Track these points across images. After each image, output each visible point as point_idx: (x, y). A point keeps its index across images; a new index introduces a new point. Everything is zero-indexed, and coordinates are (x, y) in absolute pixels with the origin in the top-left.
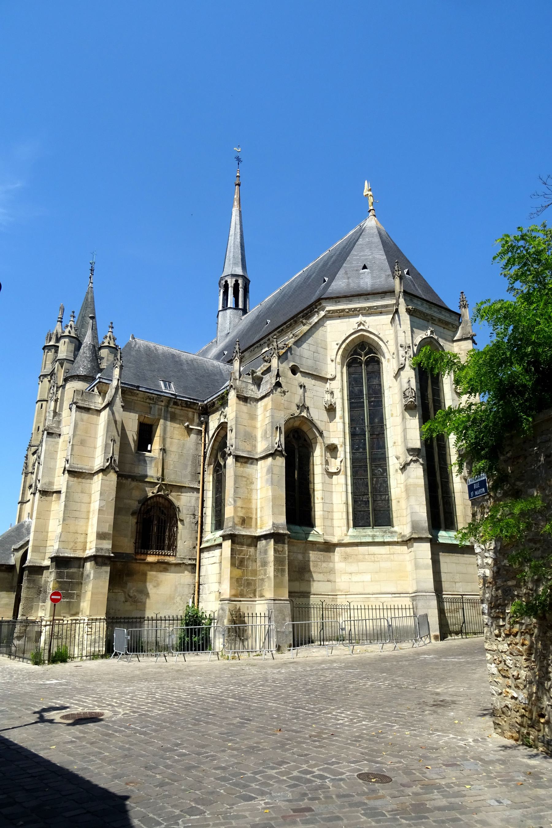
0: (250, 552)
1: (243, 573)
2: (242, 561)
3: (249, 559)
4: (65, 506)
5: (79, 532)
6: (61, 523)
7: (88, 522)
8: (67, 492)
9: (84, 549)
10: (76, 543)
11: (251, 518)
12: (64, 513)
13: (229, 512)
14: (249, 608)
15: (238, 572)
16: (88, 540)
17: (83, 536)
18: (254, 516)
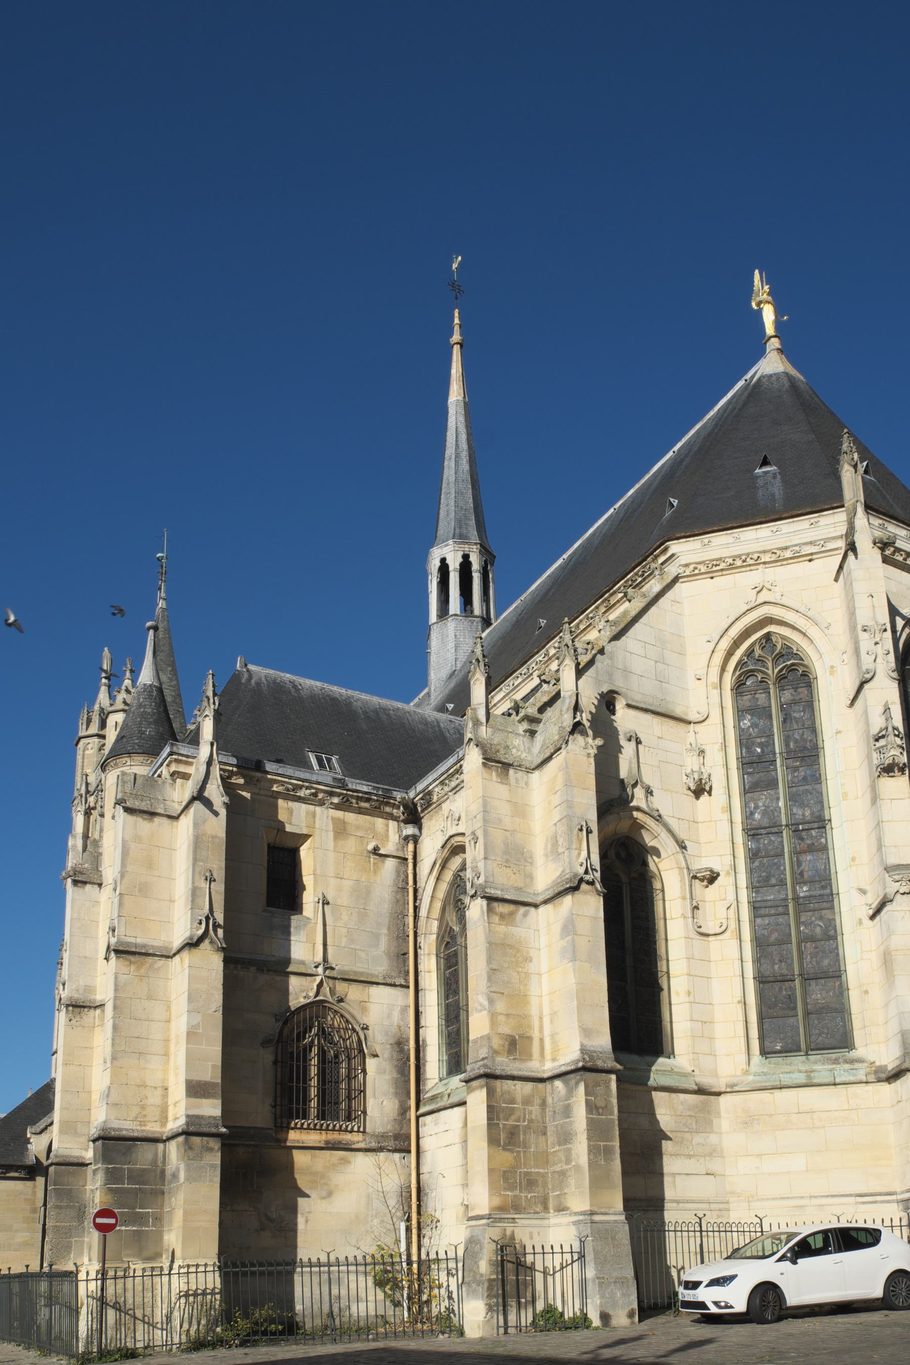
0: (530, 1113)
1: (517, 1158)
2: (513, 1133)
3: (528, 1127)
4: (115, 1027)
5: (148, 1083)
6: (109, 1064)
7: (167, 1062)
8: (116, 998)
9: (164, 1120)
10: (143, 1107)
11: (530, 1039)
12: (113, 1045)
13: (478, 1025)
14: (535, 1235)
15: (506, 1158)
16: (171, 1100)
17: (159, 1092)
18: (536, 1035)
